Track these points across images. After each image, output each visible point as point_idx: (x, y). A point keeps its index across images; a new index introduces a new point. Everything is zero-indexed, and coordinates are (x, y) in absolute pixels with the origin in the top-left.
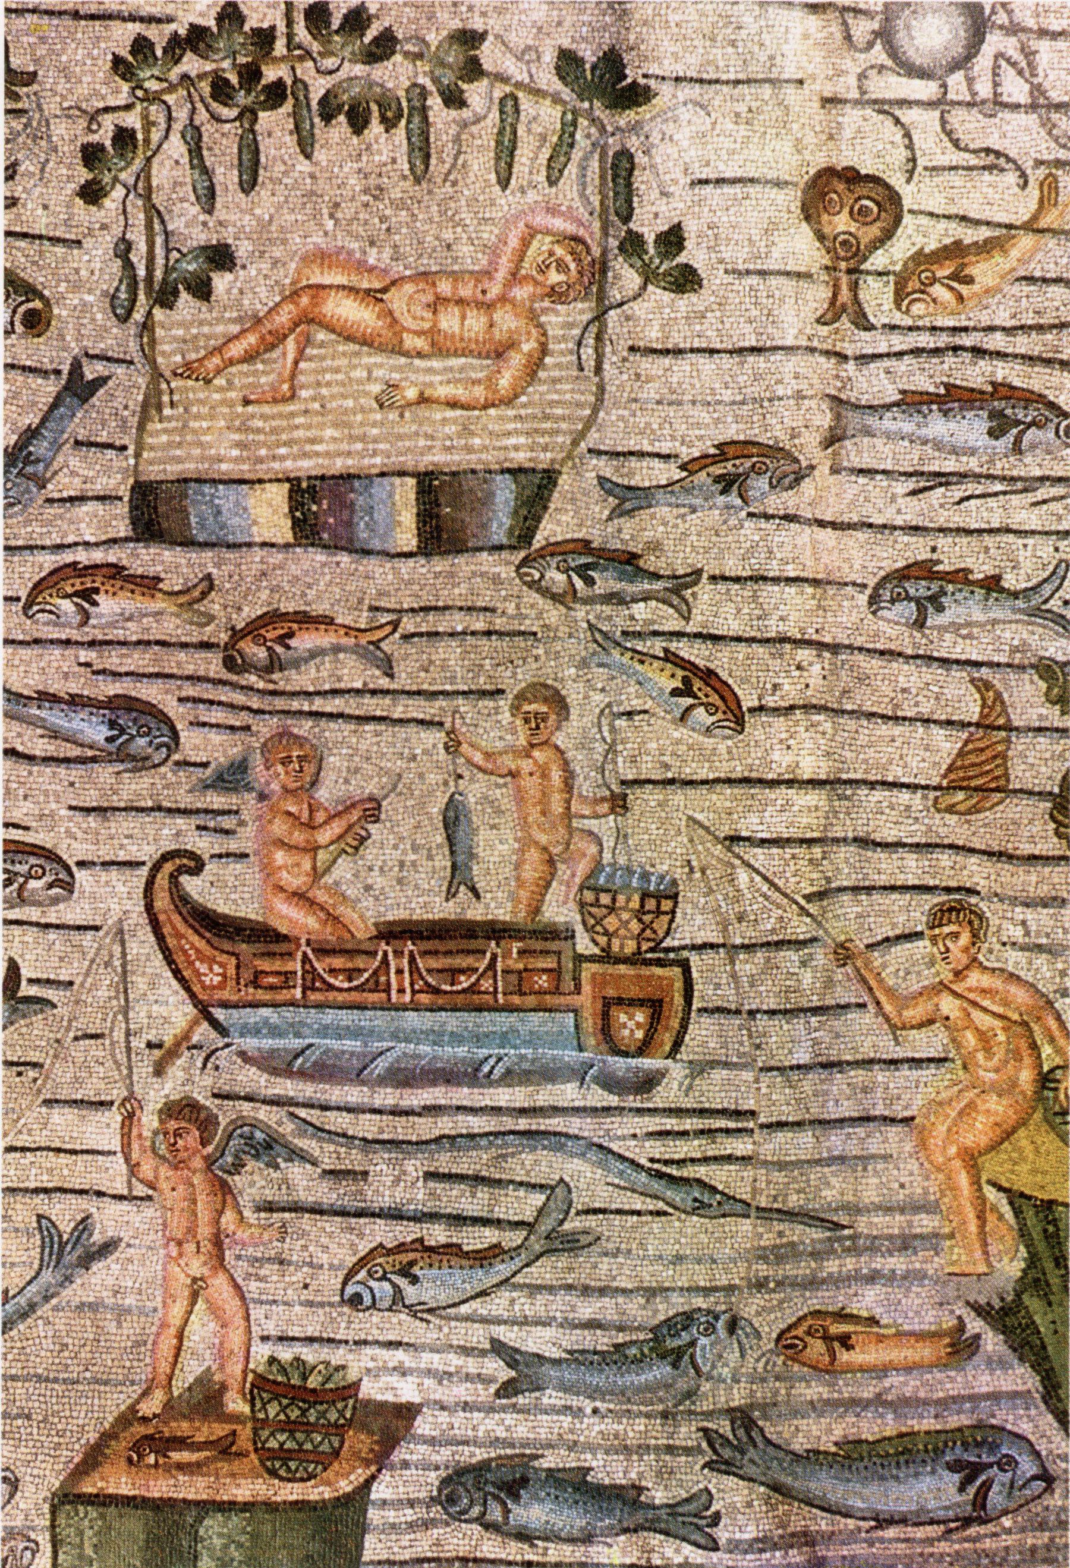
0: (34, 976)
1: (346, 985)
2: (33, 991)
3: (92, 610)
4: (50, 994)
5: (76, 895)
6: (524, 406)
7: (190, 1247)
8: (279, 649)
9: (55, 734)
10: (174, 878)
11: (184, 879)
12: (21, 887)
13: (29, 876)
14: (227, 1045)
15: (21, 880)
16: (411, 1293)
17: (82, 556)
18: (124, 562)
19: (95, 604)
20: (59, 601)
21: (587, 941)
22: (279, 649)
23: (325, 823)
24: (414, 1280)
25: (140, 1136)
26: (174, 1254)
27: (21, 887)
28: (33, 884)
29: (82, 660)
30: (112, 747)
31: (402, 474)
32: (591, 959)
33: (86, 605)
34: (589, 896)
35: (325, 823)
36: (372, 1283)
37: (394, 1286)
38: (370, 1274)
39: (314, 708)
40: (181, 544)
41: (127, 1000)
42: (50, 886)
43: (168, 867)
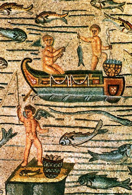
3: (10, 12)
11: (28, 63)
20: (4, 10)
21: (105, 74)
23: (55, 52)
29: (8, 21)
32: (106, 77)
33: (9, 11)
34: (105, 65)
35: (55, 52)
39: (52, 30)
42: (3, 65)
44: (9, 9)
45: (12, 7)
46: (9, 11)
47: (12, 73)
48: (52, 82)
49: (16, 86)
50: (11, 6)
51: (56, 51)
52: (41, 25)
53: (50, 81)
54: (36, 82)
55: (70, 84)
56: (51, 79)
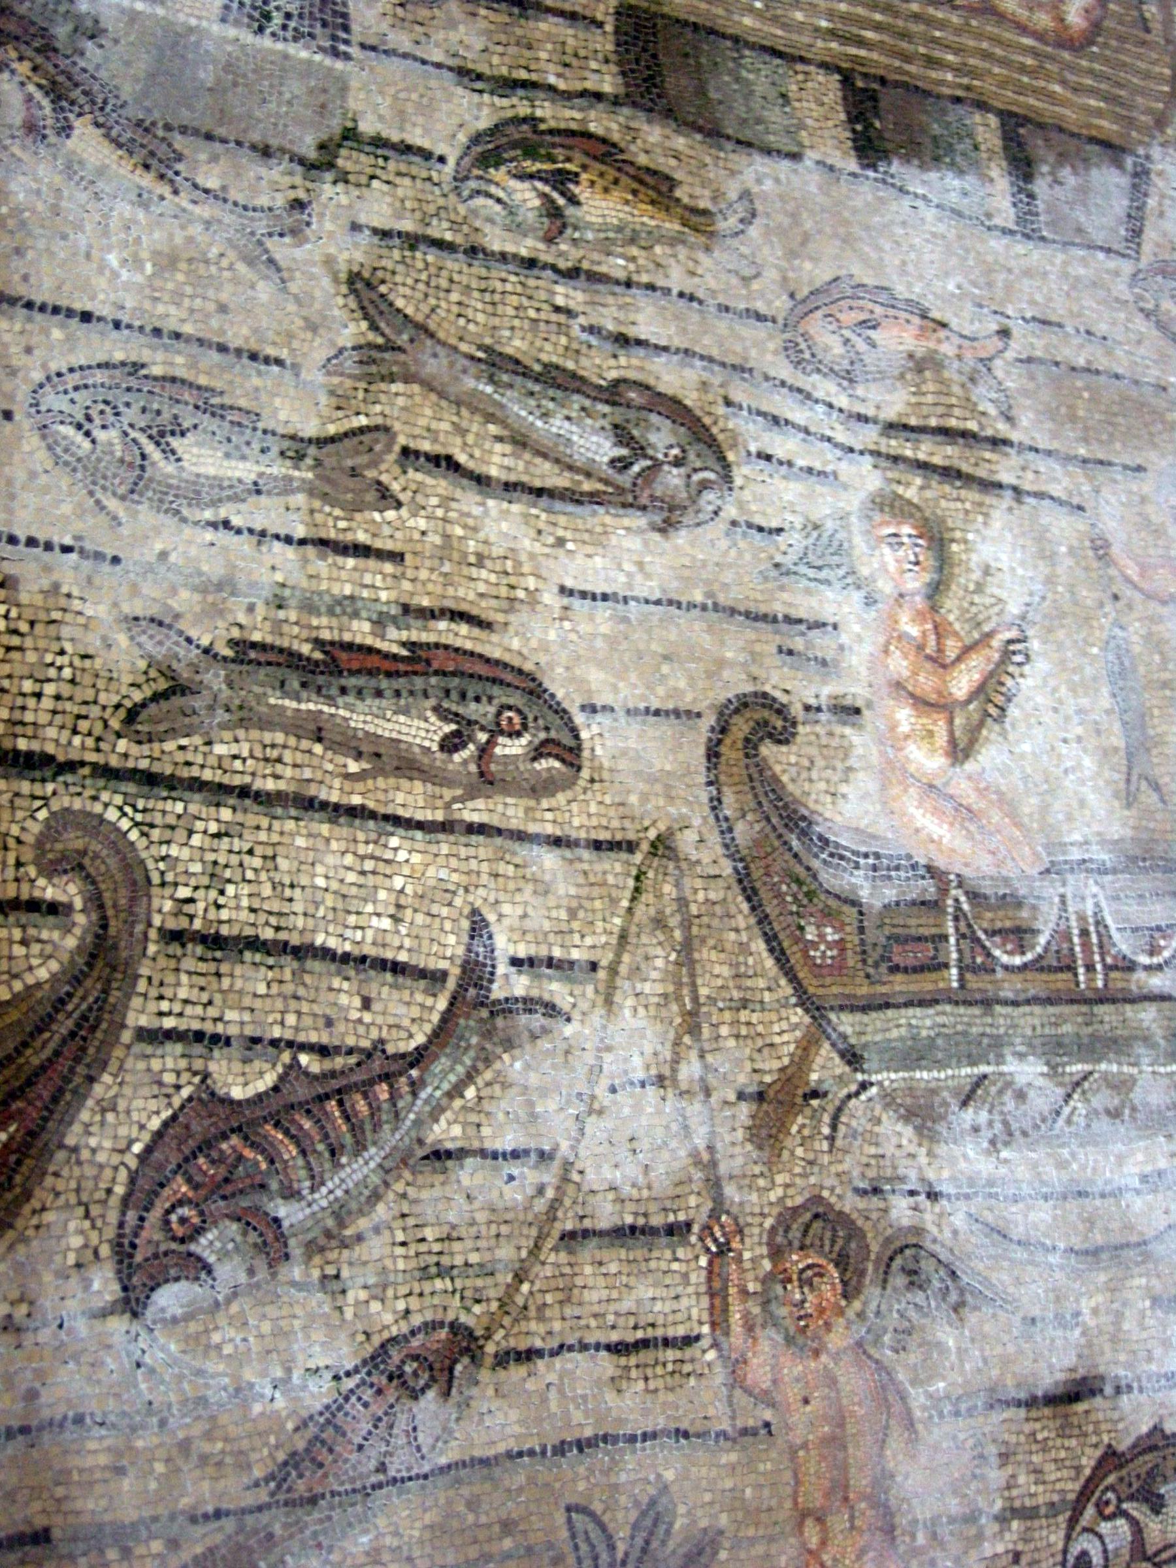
0: (522, 952)
1: (1017, 960)
2: (521, 985)
3: (570, 211)
4: (556, 990)
5: (585, 774)
6: (1093, 58)
7: (838, 1522)
8: (861, 346)
9: (520, 441)
10: (750, 745)
11: (767, 750)
12: (484, 751)
13: (496, 731)
14: (864, 1086)
15: (483, 737)
16: (1154, 1528)
17: (547, 111)
18: (616, 137)
19: (573, 201)
20: (514, 184)
22: (861, 346)
23: (959, 659)
24: (1157, 1505)
25: (744, 1292)
26: (814, 1542)
27: (484, 751)
28: (510, 748)
29: (560, 301)
30: (625, 480)
31: (982, 106)
33: (561, 201)
35: (959, 659)
36: (1105, 1527)
37: (1134, 1523)
38: (1100, 1506)
39: (921, 456)
40: (700, 130)
41: (695, 999)
42: (538, 752)
43: (741, 727)
44: (561, 179)
45: (584, 167)
46: (561, 201)
47: (631, 847)
48: (966, 945)
49: (679, 998)
50: (579, 157)
51: (967, 650)
52: (825, 388)
53: (952, 940)
54: (840, 944)
55: (1090, 968)
56: (956, 919)
